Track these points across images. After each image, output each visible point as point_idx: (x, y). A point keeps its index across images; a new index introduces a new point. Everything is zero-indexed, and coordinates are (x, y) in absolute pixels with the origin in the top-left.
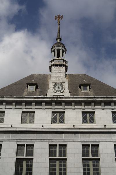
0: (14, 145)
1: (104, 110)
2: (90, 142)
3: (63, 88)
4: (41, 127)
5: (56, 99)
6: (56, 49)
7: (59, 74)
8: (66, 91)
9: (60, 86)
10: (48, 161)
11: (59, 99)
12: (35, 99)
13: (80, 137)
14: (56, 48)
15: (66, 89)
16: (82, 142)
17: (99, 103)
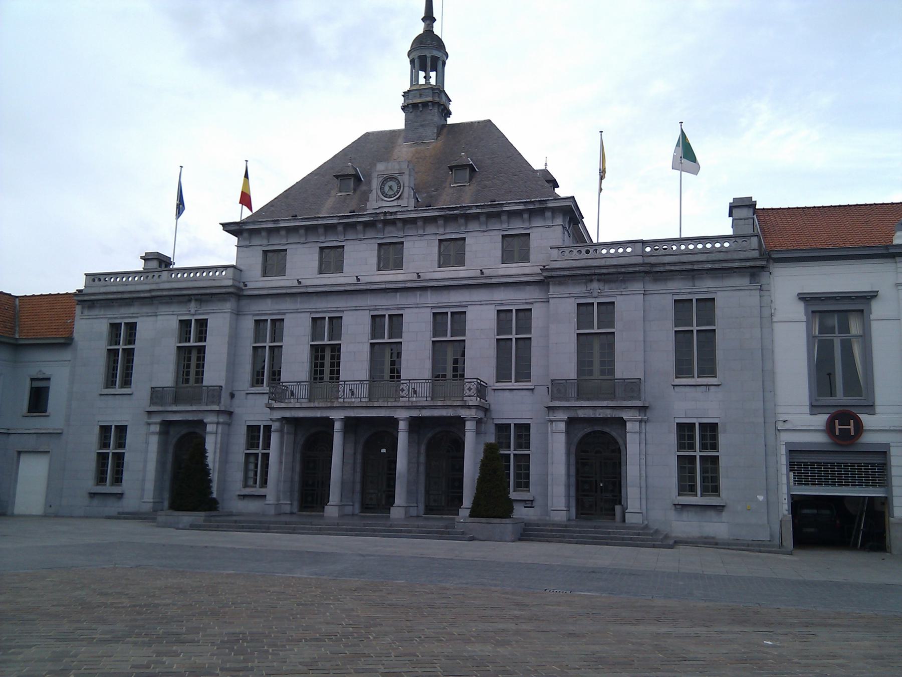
3: (400, 188)
5: (382, 218)
6: (417, 56)
7: (421, 130)
8: (406, 195)
9: (392, 183)
10: (367, 348)
11: (389, 217)
12: (341, 221)
13: (431, 299)
15: (406, 189)
16: (432, 308)
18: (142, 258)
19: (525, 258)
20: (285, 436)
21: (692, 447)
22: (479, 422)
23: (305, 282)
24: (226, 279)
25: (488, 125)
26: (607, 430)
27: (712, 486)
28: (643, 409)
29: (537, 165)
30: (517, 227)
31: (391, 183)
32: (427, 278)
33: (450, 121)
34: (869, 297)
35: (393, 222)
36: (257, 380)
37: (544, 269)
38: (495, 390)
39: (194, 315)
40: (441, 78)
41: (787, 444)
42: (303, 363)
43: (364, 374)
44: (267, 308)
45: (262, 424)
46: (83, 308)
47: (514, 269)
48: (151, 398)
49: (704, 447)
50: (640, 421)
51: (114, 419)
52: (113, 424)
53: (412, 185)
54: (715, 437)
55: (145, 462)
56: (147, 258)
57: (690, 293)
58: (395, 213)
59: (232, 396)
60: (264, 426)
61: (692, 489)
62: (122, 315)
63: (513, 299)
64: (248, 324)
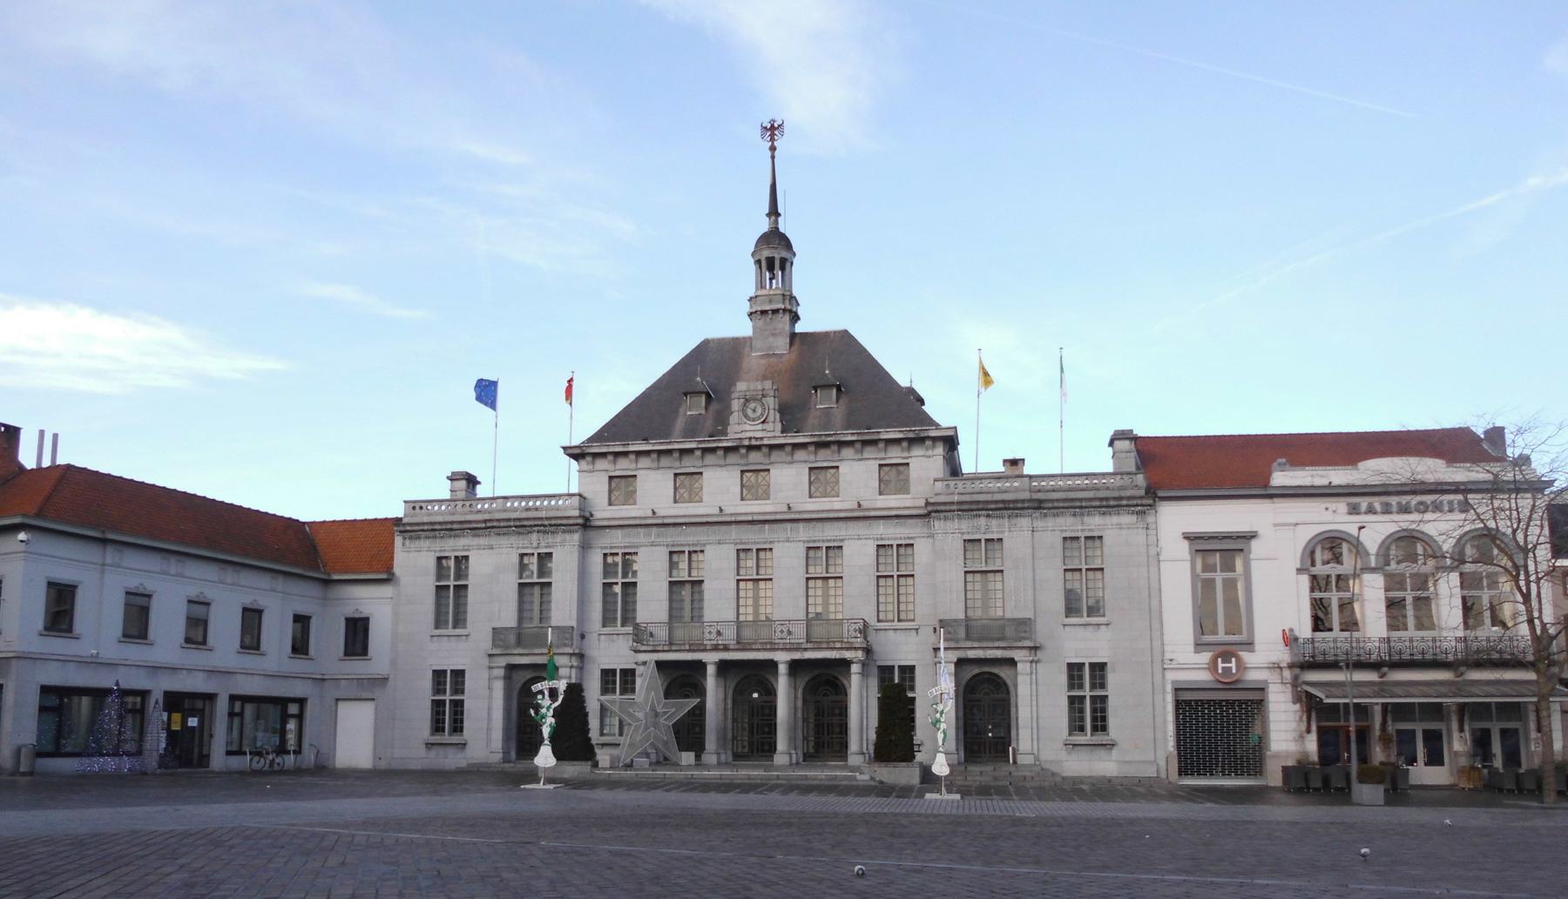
0: (662, 554)
1: (861, 462)
4: (716, 511)
7: (771, 339)
8: (771, 418)
11: (754, 442)
12: (700, 446)
14: (766, 253)
15: (772, 412)
17: (850, 444)
18: (448, 478)
19: (904, 488)
21: (1081, 687)
22: (864, 664)
23: (660, 512)
24: (571, 509)
25: (845, 337)
26: (995, 670)
27: (1100, 724)
28: (1035, 649)
29: (903, 382)
30: (895, 455)
31: (752, 405)
32: (800, 509)
33: (800, 328)
34: (1250, 536)
35: (758, 448)
36: (608, 620)
37: (927, 504)
38: (877, 630)
40: (787, 281)
41: (1174, 682)
42: (661, 601)
44: (617, 540)
45: (618, 667)
46: (405, 539)
47: (893, 501)
48: (494, 640)
49: (1093, 687)
50: (1031, 662)
51: (449, 664)
52: (449, 668)
53: (777, 408)
54: (1103, 677)
55: (489, 710)
56: (453, 478)
58: (762, 438)
59: (583, 637)
60: (621, 670)
61: (1082, 729)
62: (452, 546)
63: (893, 533)
64: (596, 560)
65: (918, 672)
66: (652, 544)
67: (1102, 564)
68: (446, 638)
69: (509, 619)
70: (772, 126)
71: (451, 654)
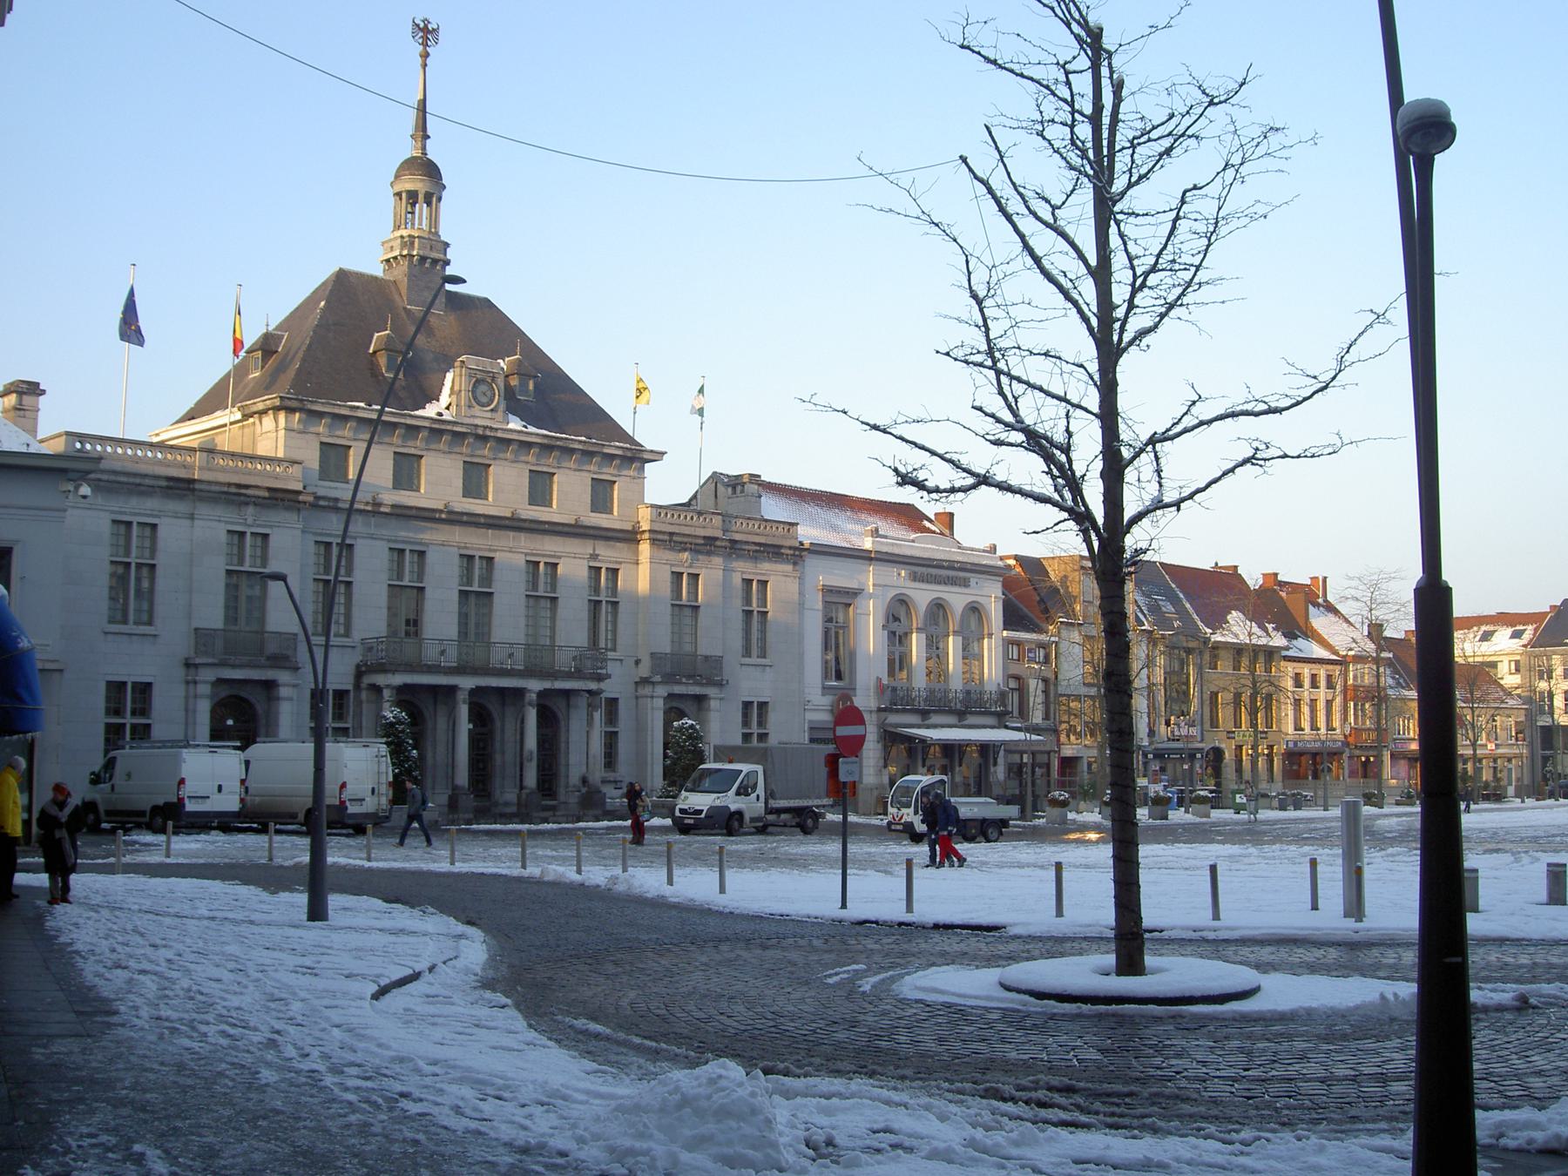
0: (381, 549)
2: (544, 556)
20: (365, 706)
39: (249, 526)
41: (810, 721)
43: (453, 632)
52: (130, 680)
57: (754, 573)
62: (137, 508)
65: (621, 702)
66: (372, 537)
67: (152, 557)
68: (349, 649)
69: (212, 615)
70: (426, 26)
71: (135, 663)
